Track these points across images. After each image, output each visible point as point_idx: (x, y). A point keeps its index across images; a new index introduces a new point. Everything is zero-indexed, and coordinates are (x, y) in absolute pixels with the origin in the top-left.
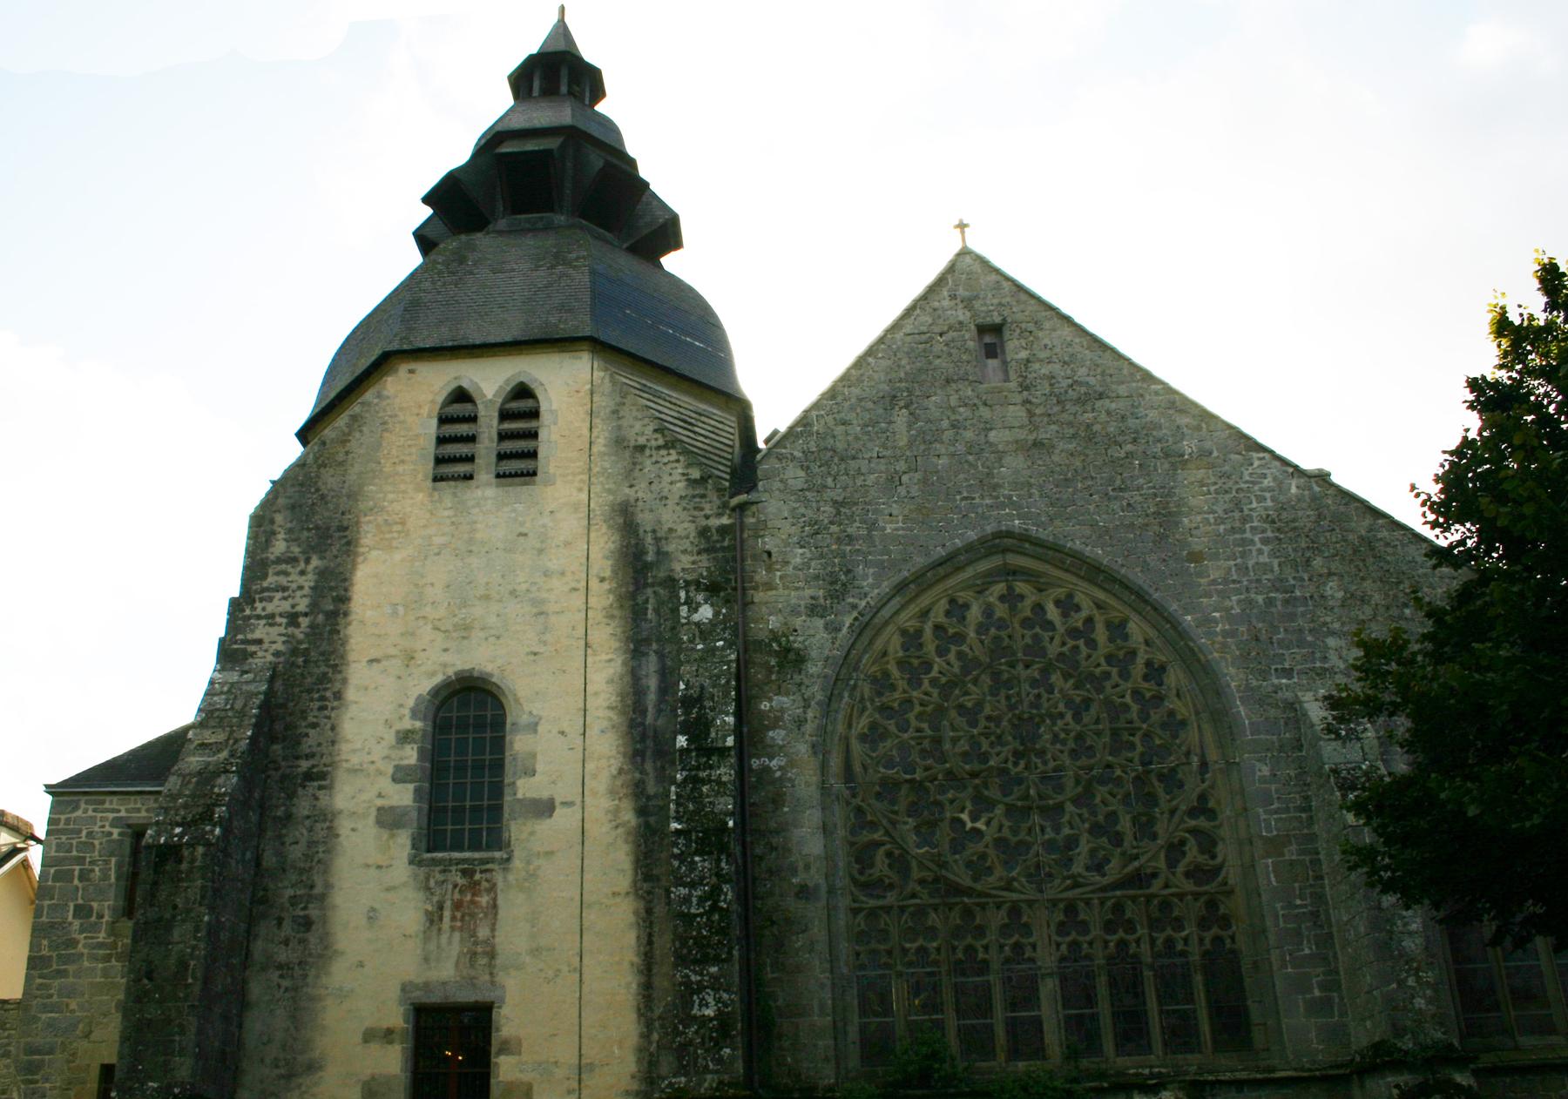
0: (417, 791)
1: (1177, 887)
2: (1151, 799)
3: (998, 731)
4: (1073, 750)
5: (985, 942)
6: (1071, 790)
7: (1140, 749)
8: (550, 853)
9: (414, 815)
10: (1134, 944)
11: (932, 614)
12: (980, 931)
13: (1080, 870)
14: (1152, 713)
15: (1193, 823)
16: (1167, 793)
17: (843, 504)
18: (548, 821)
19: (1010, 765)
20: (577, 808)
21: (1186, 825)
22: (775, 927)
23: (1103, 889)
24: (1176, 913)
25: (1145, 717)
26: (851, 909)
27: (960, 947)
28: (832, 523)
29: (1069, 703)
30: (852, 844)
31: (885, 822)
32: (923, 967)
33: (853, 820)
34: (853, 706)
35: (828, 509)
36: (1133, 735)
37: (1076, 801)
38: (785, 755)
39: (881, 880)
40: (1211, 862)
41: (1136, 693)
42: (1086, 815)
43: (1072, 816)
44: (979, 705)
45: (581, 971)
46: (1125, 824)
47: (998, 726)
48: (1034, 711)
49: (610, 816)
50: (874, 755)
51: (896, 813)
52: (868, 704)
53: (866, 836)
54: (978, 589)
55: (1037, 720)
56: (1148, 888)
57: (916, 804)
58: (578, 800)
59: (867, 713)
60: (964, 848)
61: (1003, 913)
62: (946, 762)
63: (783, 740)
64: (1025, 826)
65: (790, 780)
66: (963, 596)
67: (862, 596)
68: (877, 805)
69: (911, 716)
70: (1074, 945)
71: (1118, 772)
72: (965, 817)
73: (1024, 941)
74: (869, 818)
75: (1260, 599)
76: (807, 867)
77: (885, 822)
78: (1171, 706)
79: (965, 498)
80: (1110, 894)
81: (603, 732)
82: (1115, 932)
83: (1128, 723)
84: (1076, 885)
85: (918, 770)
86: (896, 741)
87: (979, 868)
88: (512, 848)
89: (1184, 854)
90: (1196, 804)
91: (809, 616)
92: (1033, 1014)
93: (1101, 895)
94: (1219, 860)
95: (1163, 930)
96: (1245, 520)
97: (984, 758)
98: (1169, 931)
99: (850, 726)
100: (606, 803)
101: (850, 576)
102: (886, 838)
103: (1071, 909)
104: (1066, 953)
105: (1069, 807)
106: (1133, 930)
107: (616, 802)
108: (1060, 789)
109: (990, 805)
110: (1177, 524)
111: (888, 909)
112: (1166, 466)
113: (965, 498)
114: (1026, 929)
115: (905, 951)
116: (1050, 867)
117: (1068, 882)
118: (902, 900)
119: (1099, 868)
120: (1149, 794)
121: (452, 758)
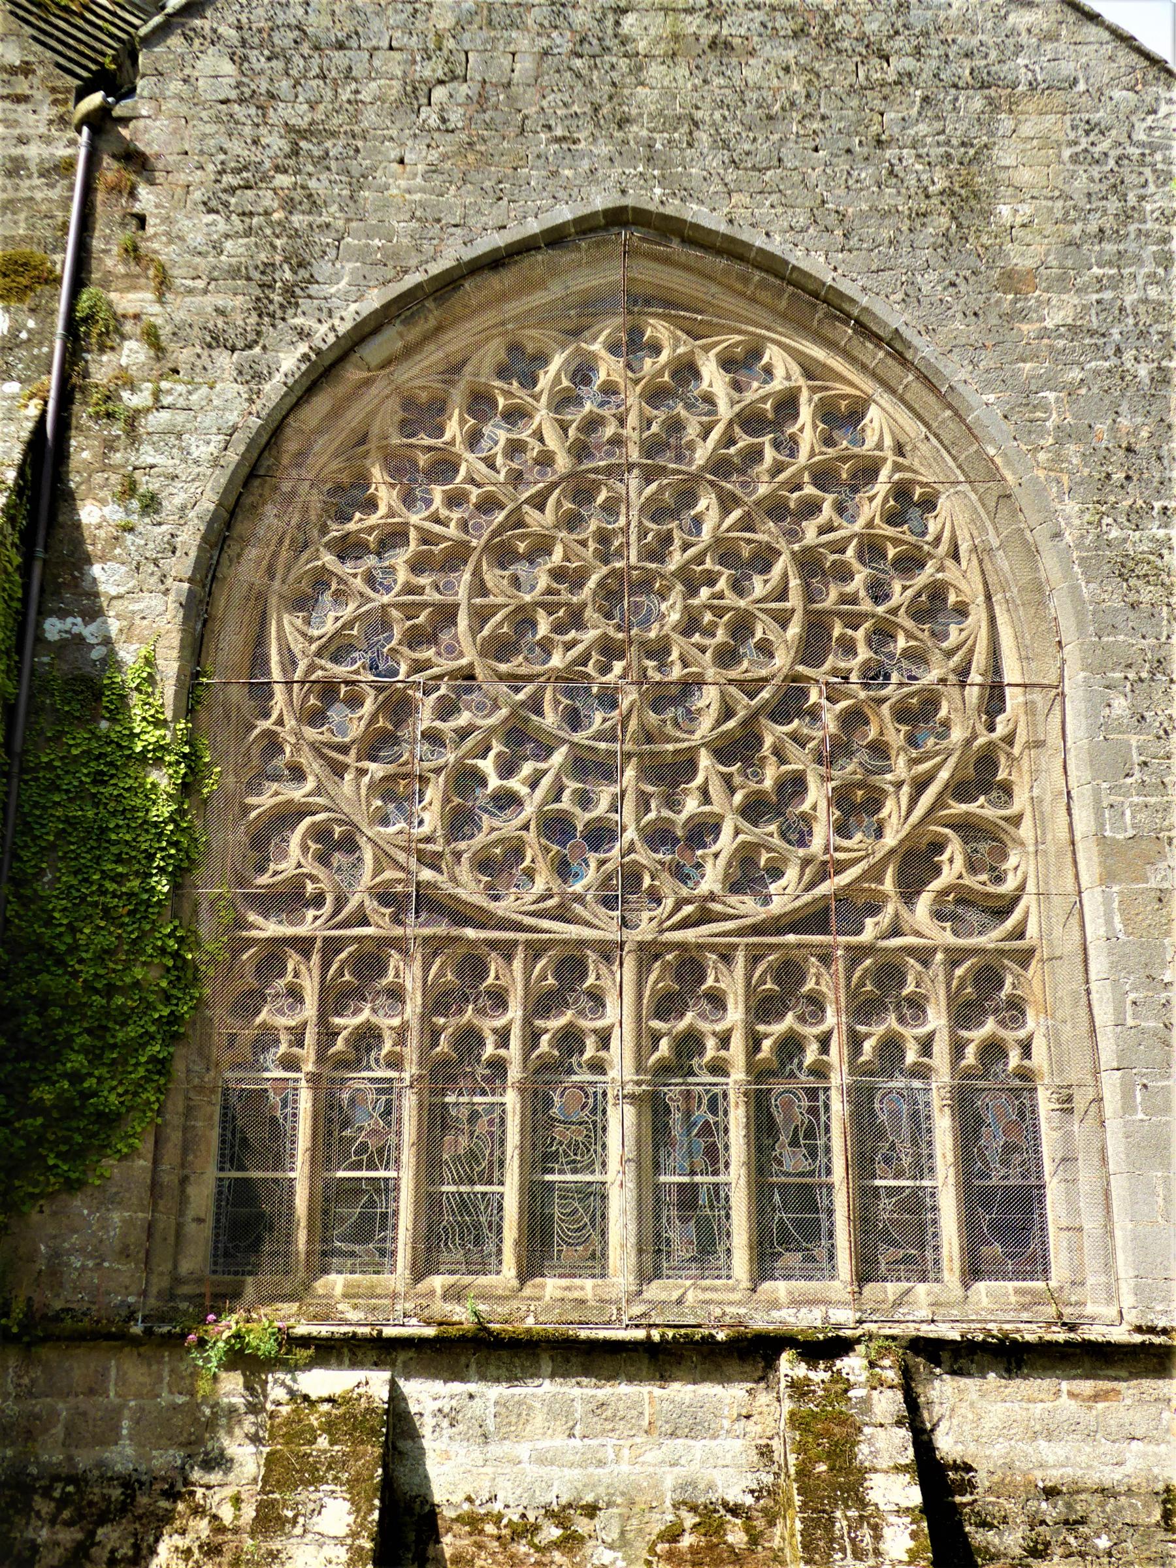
1: (918, 934)
11: (468, 369)
17: (304, 134)
25: (878, 592)
28: (278, 169)
35: (277, 143)
37: (724, 752)
40: (991, 889)
54: (570, 325)
66: (533, 338)
67: (324, 316)
75: (1143, 371)
79: (558, 140)
84: (704, 917)
89: (937, 871)
91: (210, 346)
92: (589, 1178)
94: (1009, 886)
96: (1127, 216)
99: (271, 573)
101: (303, 274)
110: (986, 214)
111: (303, 945)
112: (978, 103)
113: (558, 140)
117: (688, 909)
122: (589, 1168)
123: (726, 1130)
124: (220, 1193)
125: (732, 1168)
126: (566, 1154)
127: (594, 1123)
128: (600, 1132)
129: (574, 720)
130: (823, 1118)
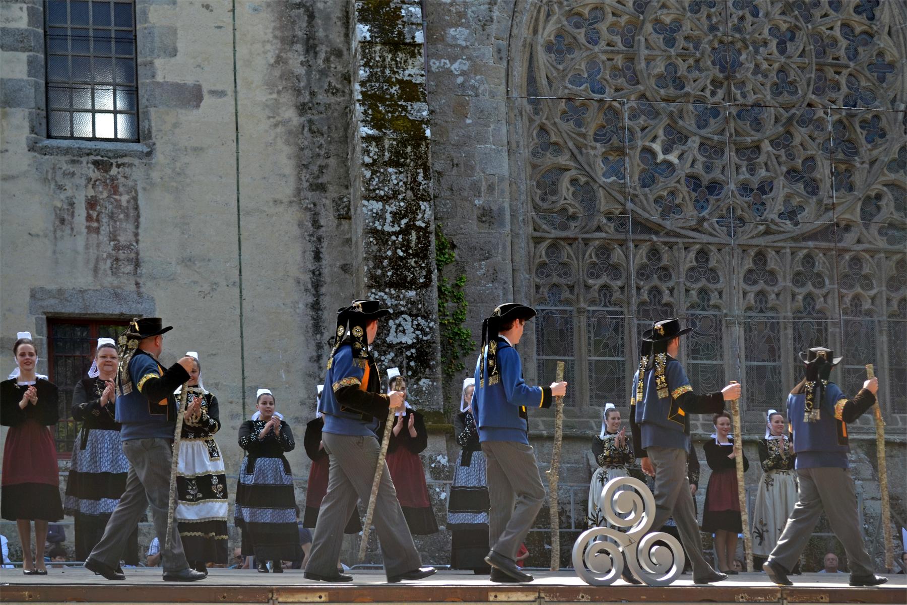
0: (31, 62)
1: (870, 242)
2: (852, 149)
3: (698, 55)
4: (775, 84)
5: (671, 284)
6: (771, 129)
7: (844, 89)
8: (197, 150)
9: (31, 92)
10: (822, 299)
12: (666, 273)
13: (774, 216)
14: (860, 49)
15: (891, 177)
16: (869, 142)
18: (195, 112)
19: (708, 93)
20: (229, 100)
21: (884, 178)
22: (456, 251)
23: (794, 239)
24: (866, 270)
25: (853, 55)
26: (533, 238)
27: (646, 288)
29: (774, 30)
30: (534, 166)
31: (571, 144)
32: (605, 306)
33: (536, 141)
34: (540, 7)
36: (838, 73)
37: (774, 143)
38: (469, 59)
39: (564, 210)
41: (846, 26)
42: (784, 158)
43: (769, 157)
44: (677, 25)
45: (241, 285)
46: (824, 171)
47: (696, 48)
48: (737, 36)
49: (268, 112)
50: (561, 67)
51: (584, 136)
52: (556, 6)
53: (549, 159)
55: (739, 45)
56: (840, 241)
57: (604, 127)
58: (230, 89)
59: (554, 19)
60: (653, 182)
61: (692, 255)
62: (638, 83)
63: (465, 40)
64: (718, 163)
65: (473, 87)
68: (565, 126)
69: (603, 27)
70: (761, 294)
71: (820, 113)
72: (657, 147)
73: (711, 286)
74: (554, 139)
76: (491, 188)
77: (571, 144)
78: (882, 45)
80: (803, 244)
81: (255, 10)
82: (803, 285)
83: (833, 59)
84: (767, 232)
85: (607, 90)
86: (584, 54)
87: (669, 208)
88: (154, 140)
90: (897, 156)
92: (715, 362)
93: (793, 245)
95: (852, 287)
97: (679, 84)
98: (858, 289)
99: (535, 32)
100: (263, 96)
102: (572, 164)
103: (760, 257)
104: (753, 302)
105: (766, 146)
106: (822, 284)
107: (275, 96)
108: (758, 124)
109: (683, 138)
111: (571, 241)
114: (713, 275)
115: (588, 287)
116: (743, 211)
117: (762, 228)
118: (587, 232)
119: (792, 215)
120: (849, 141)
121: (69, 25)
122: (714, 357)
123: (779, 340)
124: (539, 366)
125: (782, 359)
126: (703, 351)
127: (716, 335)
128: (719, 340)
129: (702, 123)
130: (824, 335)
